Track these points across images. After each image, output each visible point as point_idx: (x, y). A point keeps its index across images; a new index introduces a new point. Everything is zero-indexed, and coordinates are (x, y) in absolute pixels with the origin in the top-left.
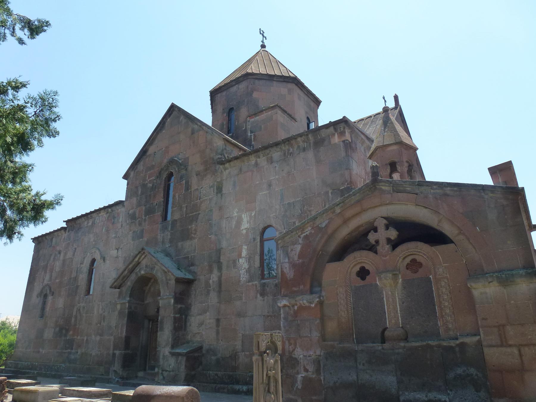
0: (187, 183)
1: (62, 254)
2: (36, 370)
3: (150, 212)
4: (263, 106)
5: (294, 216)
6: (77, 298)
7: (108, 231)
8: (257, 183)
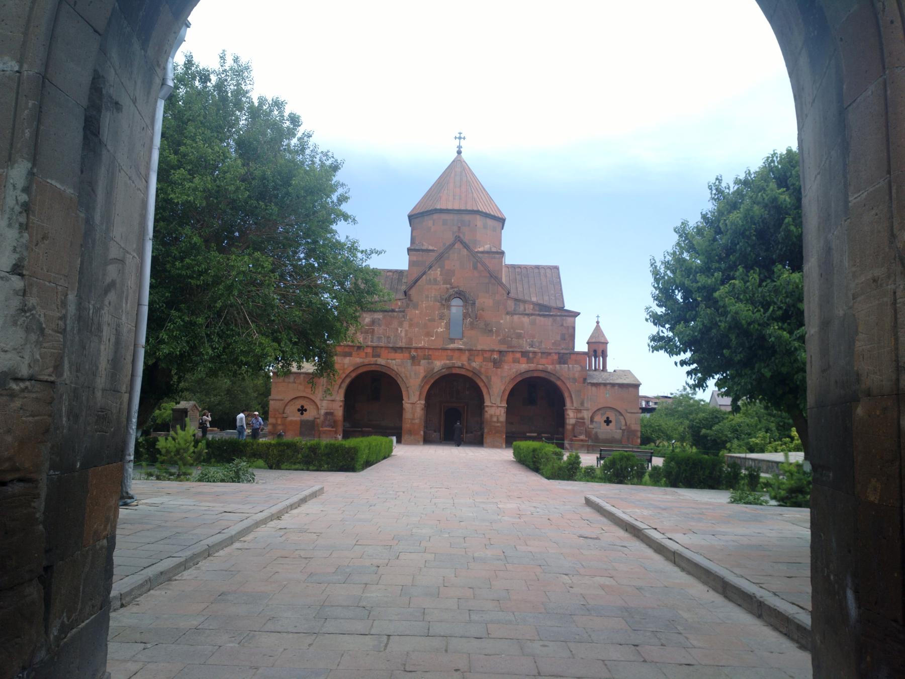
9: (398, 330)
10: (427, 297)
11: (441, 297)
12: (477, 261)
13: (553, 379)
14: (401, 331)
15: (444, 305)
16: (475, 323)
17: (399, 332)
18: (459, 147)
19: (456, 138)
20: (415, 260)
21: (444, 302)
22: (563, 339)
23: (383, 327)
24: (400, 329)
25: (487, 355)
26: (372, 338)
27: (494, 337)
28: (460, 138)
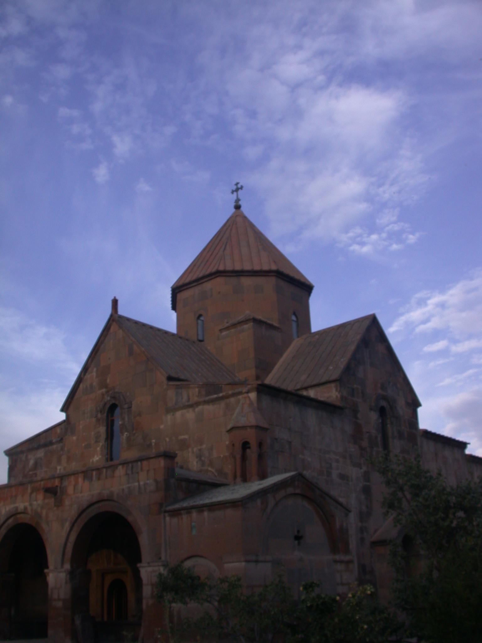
9: (56, 469)
14: (60, 469)
18: (238, 200)
19: (233, 192)
24: (59, 468)
28: (237, 190)
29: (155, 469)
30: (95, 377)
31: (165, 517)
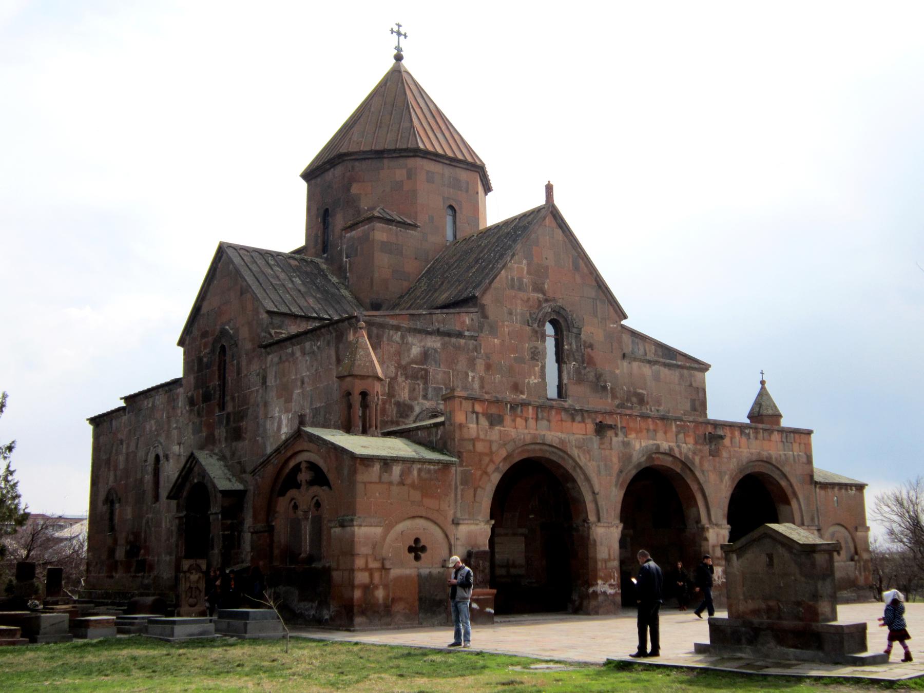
0: (238, 364)
1: (125, 446)
2: (110, 598)
3: (207, 398)
4: (366, 208)
5: (319, 424)
6: (145, 508)
7: (168, 417)
8: (293, 377)
10: (511, 314)
11: (530, 314)
12: (579, 253)
13: (776, 476)
14: (473, 378)
15: (536, 332)
16: (583, 372)
17: (470, 378)
18: (399, 49)
20: (385, 240)
21: (536, 325)
22: (694, 409)
23: (443, 368)
25: (701, 431)
26: (425, 389)
27: (610, 401)
29: (805, 444)
30: (525, 272)
31: (815, 487)
